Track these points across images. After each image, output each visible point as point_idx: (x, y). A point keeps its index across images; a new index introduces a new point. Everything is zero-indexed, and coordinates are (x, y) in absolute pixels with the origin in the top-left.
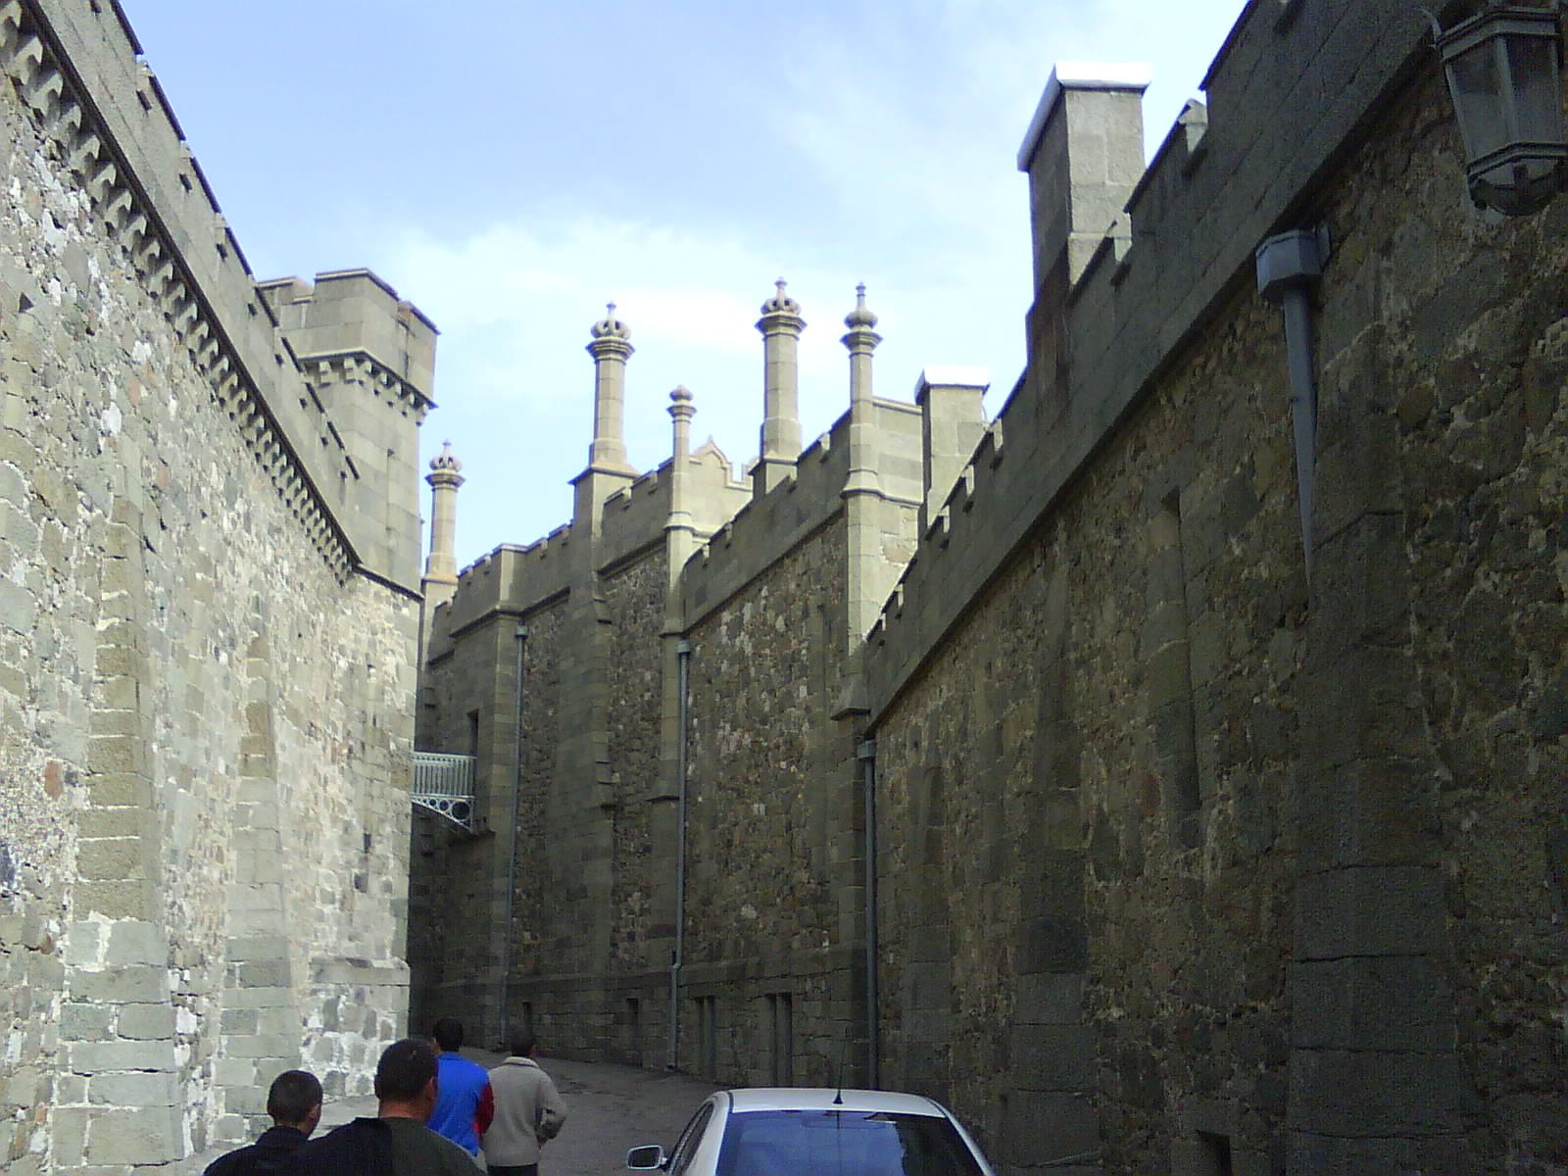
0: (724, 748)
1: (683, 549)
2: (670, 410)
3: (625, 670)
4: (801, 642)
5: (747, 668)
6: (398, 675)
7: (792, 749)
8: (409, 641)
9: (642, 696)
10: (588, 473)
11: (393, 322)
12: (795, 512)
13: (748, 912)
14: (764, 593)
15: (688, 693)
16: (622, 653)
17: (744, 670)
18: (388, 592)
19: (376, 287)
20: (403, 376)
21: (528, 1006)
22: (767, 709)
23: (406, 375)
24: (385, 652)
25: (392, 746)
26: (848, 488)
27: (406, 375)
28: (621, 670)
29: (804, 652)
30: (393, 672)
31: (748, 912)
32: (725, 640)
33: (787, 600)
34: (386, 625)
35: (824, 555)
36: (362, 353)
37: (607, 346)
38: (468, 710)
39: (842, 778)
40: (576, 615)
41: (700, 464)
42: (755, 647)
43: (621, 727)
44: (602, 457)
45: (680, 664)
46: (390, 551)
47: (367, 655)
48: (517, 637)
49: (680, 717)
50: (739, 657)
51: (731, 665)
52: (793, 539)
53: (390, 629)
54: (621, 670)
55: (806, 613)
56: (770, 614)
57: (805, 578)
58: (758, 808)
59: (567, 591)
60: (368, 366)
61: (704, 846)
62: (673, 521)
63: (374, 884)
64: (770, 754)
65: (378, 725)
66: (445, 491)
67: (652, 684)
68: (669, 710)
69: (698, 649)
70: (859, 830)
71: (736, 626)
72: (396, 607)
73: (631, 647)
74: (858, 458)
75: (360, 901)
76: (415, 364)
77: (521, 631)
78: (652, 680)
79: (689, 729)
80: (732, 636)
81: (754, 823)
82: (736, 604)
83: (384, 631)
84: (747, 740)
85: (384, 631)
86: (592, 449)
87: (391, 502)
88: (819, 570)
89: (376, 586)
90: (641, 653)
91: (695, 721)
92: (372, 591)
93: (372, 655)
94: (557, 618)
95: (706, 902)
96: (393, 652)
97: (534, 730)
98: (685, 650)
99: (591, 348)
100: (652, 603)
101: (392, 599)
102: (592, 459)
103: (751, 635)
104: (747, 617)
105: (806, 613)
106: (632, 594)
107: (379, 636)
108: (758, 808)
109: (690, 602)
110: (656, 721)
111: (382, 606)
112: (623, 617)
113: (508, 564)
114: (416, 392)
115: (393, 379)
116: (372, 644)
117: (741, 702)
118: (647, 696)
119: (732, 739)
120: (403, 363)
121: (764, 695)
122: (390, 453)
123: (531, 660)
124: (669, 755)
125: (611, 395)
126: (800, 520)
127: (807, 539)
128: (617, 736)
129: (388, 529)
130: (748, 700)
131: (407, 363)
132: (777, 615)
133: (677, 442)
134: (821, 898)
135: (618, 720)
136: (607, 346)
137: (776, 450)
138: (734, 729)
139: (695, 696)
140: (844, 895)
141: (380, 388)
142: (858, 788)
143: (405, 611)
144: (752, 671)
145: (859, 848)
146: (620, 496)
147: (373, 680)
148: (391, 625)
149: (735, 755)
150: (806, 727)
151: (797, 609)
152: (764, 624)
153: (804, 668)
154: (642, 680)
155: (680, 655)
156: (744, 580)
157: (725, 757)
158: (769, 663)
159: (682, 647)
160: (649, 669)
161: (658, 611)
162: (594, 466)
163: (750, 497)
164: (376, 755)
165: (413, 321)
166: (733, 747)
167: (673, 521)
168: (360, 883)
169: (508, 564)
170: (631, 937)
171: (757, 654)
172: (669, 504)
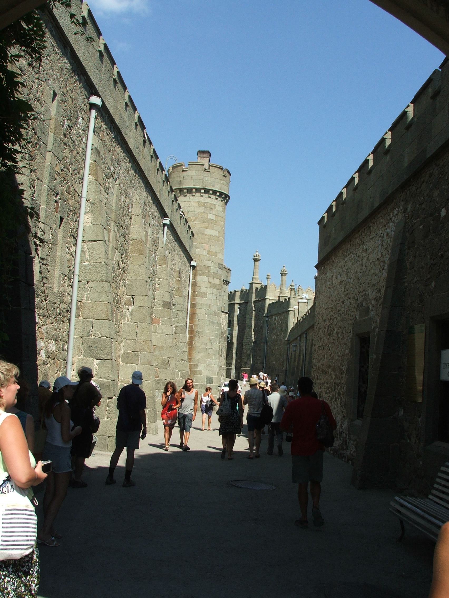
1: (268, 302)
7: (281, 341)
13: (274, 362)
17: (276, 327)
33: (282, 319)
39: (286, 349)
50: (275, 324)
58: (276, 348)
61: (268, 351)
62: (266, 297)
63: (222, 355)
70: (287, 355)
75: (221, 358)
95: (269, 360)
102: (253, 280)
108: (276, 348)
119: (274, 337)
124: (264, 336)
126: (284, 308)
140: (285, 363)
142: (287, 350)
145: (287, 357)
159: (267, 319)
164: (223, 337)
167: (266, 297)
168: (221, 356)
169: (238, 295)
170: (257, 363)
172: (266, 294)
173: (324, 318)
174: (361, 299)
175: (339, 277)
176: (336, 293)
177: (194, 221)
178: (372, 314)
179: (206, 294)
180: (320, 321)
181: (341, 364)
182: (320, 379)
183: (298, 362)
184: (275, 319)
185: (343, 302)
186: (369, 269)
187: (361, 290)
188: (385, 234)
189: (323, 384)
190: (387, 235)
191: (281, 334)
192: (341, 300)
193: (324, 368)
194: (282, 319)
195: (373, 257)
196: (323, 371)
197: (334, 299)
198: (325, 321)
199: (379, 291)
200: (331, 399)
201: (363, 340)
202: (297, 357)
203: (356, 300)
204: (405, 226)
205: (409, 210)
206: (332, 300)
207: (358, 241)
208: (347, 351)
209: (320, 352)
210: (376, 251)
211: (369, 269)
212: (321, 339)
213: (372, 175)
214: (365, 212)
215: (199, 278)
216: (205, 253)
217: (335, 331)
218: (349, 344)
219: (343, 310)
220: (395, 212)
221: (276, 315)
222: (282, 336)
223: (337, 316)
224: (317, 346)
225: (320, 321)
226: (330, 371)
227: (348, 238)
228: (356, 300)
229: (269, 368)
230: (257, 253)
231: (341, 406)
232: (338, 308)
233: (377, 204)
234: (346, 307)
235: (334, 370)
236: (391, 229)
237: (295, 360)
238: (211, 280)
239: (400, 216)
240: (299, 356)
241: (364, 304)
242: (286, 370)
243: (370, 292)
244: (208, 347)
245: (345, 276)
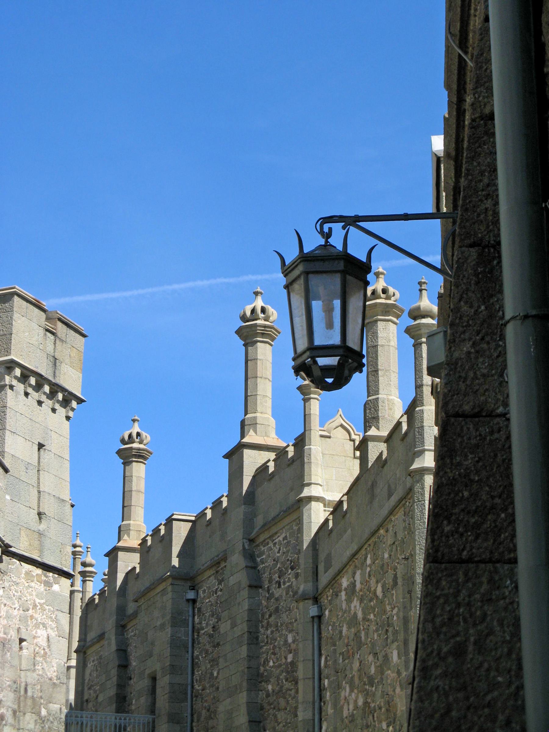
0: (345, 707)
2: (120, 452)
3: (272, 632)
4: (393, 609)
5: (359, 631)
6: (49, 646)
8: (60, 614)
9: (286, 658)
10: (241, 447)
11: (42, 331)
12: (387, 486)
14: (369, 561)
15: (320, 655)
16: (270, 616)
18: (39, 571)
19: (25, 303)
20: (51, 378)
22: (373, 670)
23: (54, 376)
24: (37, 626)
25: (44, 712)
26: (415, 466)
27: (54, 376)
28: (269, 632)
29: (395, 618)
30: (44, 644)
32: (344, 606)
34: (38, 601)
35: (405, 528)
36: (12, 361)
38: (147, 672)
40: (232, 580)
41: (329, 437)
42: (364, 613)
43: (270, 687)
44: (252, 432)
45: (313, 626)
46: (41, 534)
47: (19, 630)
48: (188, 600)
49: (314, 678)
50: (353, 621)
51: (349, 628)
52: (385, 512)
53: (41, 605)
54: (269, 632)
55: (395, 583)
56: (373, 581)
57: (394, 547)
59: (225, 559)
60: (18, 372)
62: (306, 492)
64: (375, 715)
65: (30, 693)
66: (134, 464)
67: (293, 646)
68: (302, 671)
69: (327, 613)
71: (351, 590)
72: (48, 584)
73: (277, 610)
74: (310, 475)
76: (63, 365)
77: (191, 595)
78: (294, 642)
79: (321, 689)
80: (349, 601)
82: (350, 569)
83: (35, 606)
84: (360, 702)
85: (35, 606)
86: (243, 424)
87: (41, 490)
88: (403, 541)
89: (27, 567)
90: (284, 616)
91: (326, 681)
92: (24, 571)
93: (23, 630)
94: (220, 583)
96: (44, 626)
97: (203, 690)
98: (317, 614)
99: (239, 332)
100: (292, 568)
101: (43, 578)
103: (361, 601)
104: (358, 586)
105: (395, 583)
106: (276, 561)
107: (31, 612)
109: (321, 568)
110: (296, 681)
111: (33, 584)
112: (270, 581)
113: (180, 532)
114: (64, 390)
115: (41, 380)
116: (23, 619)
117: (356, 665)
118: (290, 658)
120: (51, 364)
121: (371, 658)
122: (41, 446)
123: (200, 623)
125: (259, 374)
126: (390, 495)
128: (268, 695)
129: (39, 514)
130: (361, 662)
131: (55, 364)
132: (377, 582)
135: (268, 681)
137: (378, 429)
138: (352, 691)
139: (326, 658)
141: (30, 390)
143: (56, 587)
144: (363, 634)
146: (264, 467)
147: (25, 651)
148: (42, 601)
149: (353, 715)
150: (398, 690)
151: (389, 580)
152: (369, 590)
153: (396, 632)
154: (286, 641)
155: (313, 617)
156: (355, 547)
157: (346, 717)
158: (373, 627)
159: (313, 611)
160: (290, 631)
161: (297, 576)
162: (246, 440)
163: (356, 471)
165: (61, 328)
166: (351, 707)
167: (306, 492)
171: (365, 619)
172: (301, 476)
184: (351, 590)
222: (390, 674)
230: (259, 303)
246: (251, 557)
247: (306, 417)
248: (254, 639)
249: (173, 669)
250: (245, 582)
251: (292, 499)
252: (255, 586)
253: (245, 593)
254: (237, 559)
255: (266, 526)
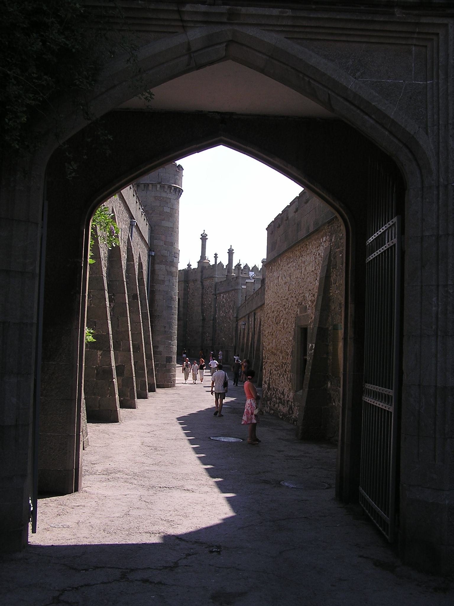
13: (224, 339)
21: (189, 349)
31: (224, 339)
33: (230, 298)
37: (204, 238)
39: (234, 326)
50: (223, 302)
68: (212, 306)
71: (223, 297)
79: (216, 310)
81: (225, 327)
119: (222, 314)
127: (233, 290)
133: (216, 262)
134: (232, 339)
136: (204, 238)
173: (272, 310)
174: (301, 299)
175: (284, 278)
176: (282, 290)
177: (151, 214)
178: (309, 312)
179: (163, 281)
180: (269, 311)
181: (287, 347)
182: (270, 359)
183: (248, 339)
184: (223, 297)
185: (287, 299)
186: (306, 277)
187: (301, 292)
188: (318, 254)
189: (273, 363)
190: (319, 254)
191: (229, 311)
192: (286, 298)
193: (273, 350)
194: (230, 298)
195: (310, 268)
196: (272, 352)
197: (280, 296)
198: (273, 312)
199: (314, 295)
200: (280, 375)
201: (304, 331)
202: (246, 335)
203: (297, 299)
204: (330, 252)
205: (333, 240)
206: (279, 296)
207: (298, 253)
208: (291, 338)
209: (270, 337)
210: (311, 265)
211: (306, 277)
212: (270, 326)
213: (308, 204)
214: (303, 233)
215: (157, 267)
216: (162, 243)
217: (282, 322)
218: (293, 333)
219: (287, 305)
220: (324, 239)
221: (224, 293)
223: (283, 309)
224: (267, 332)
225: (269, 311)
226: (278, 353)
227: (290, 249)
228: (297, 299)
229: (219, 344)
231: (288, 381)
232: (284, 303)
233: (311, 229)
234: (290, 303)
235: (281, 352)
236: (322, 251)
237: (244, 337)
238: (168, 268)
239: (327, 243)
240: (248, 333)
241: (303, 304)
242: (235, 347)
243: (307, 295)
244: (166, 329)
245: (289, 279)
246: (202, 282)
247: (216, 262)
248: (202, 298)
249: (184, 299)
250: (201, 287)
251: (211, 275)
252: (203, 288)
253: (201, 289)
254: (199, 282)
255: (205, 278)
